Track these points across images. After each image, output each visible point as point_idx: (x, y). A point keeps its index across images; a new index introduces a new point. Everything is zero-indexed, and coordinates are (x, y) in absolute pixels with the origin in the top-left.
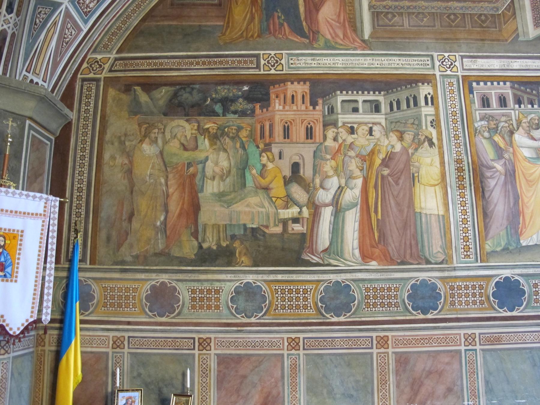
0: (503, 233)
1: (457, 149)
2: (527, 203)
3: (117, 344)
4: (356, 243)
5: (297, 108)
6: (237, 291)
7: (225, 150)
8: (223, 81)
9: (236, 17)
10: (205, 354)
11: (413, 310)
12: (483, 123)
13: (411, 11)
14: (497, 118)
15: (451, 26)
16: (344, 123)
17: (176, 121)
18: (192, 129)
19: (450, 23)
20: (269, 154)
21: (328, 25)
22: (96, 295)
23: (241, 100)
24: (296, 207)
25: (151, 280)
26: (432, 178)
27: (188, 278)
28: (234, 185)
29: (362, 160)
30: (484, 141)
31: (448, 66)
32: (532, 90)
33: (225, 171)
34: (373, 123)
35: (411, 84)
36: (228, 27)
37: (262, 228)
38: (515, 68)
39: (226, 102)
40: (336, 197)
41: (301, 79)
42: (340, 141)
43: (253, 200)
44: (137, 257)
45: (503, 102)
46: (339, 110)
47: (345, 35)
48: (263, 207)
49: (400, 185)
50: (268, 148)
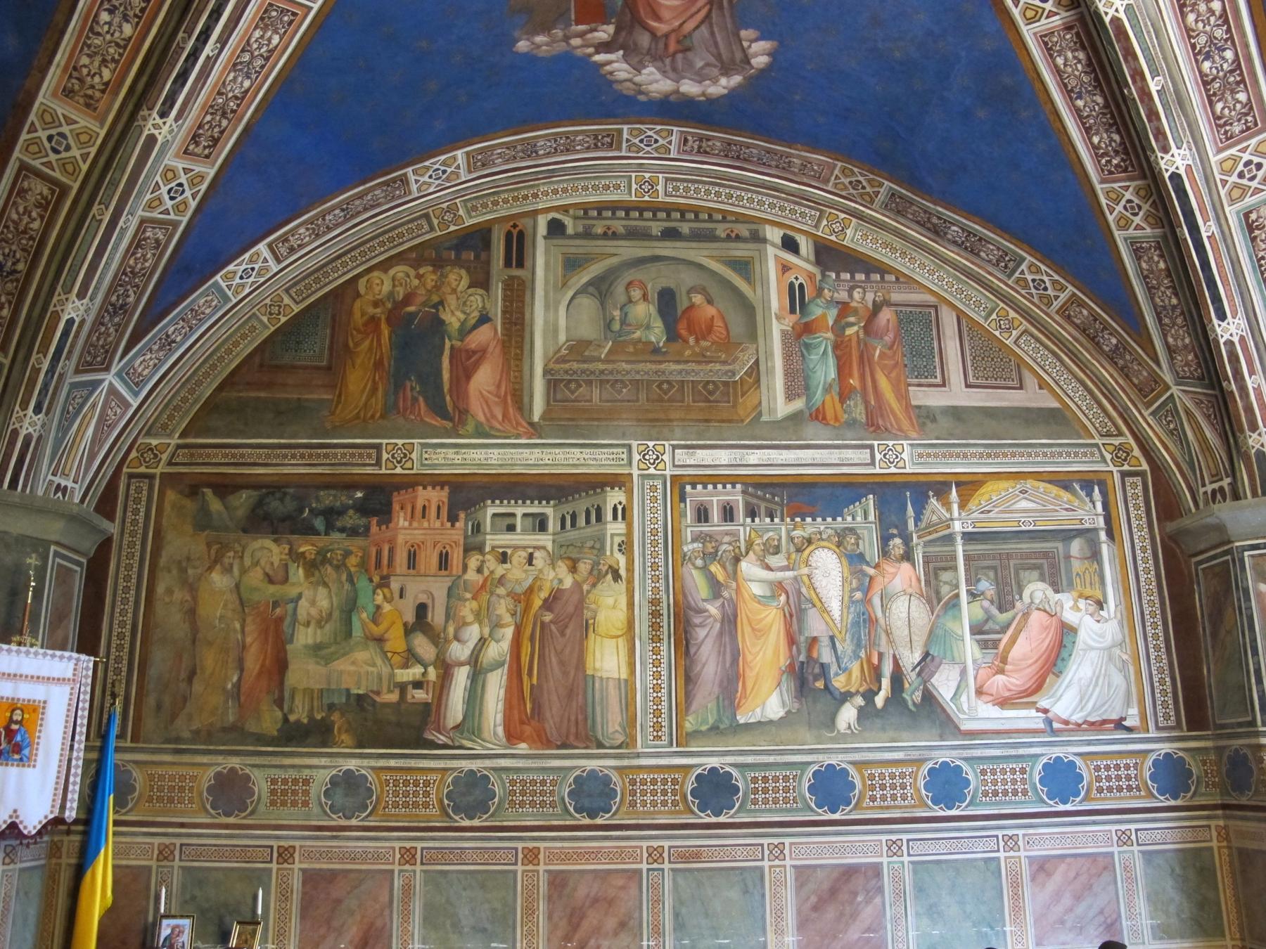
0: (712, 705)
3: (165, 854)
4: (500, 717)
6: (334, 782)
7: (325, 585)
10: (286, 869)
11: (576, 812)
12: (695, 545)
14: (718, 538)
16: (493, 548)
17: (260, 541)
18: (281, 553)
20: (386, 590)
22: (137, 786)
23: (351, 512)
25: (216, 764)
27: (266, 763)
28: (335, 634)
30: (694, 572)
31: (652, 461)
32: (774, 495)
34: (534, 548)
35: (594, 488)
36: (339, 402)
37: (371, 695)
38: (752, 462)
39: (331, 515)
40: (476, 652)
41: (437, 481)
42: (486, 572)
43: (361, 655)
44: (197, 732)
45: (728, 513)
46: (488, 529)
47: (505, 416)
48: (374, 665)
50: (384, 583)
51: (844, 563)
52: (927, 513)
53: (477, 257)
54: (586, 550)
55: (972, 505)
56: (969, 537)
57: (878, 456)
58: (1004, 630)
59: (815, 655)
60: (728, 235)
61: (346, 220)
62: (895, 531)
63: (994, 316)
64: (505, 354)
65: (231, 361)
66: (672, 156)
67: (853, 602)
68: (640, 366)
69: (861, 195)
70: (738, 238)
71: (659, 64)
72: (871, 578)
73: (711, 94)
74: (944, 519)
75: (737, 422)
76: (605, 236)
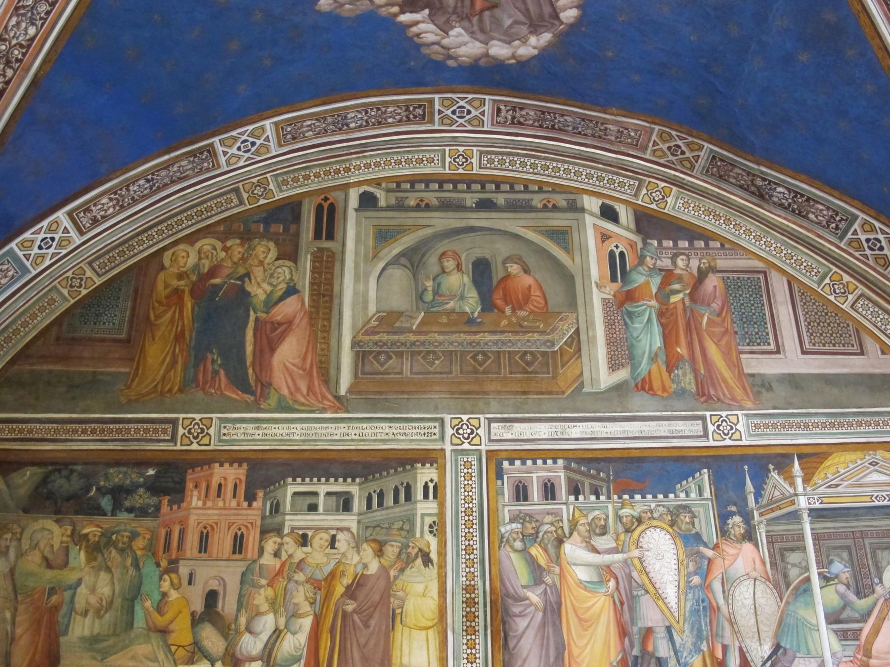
1: (468, 570)
2: (579, 655)
5: (224, 504)
7: (109, 570)
8: (118, 460)
9: (150, 360)
12: (514, 526)
13: (416, 349)
14: (538, 517)
15: (476, 372)
16: (293, 529)
17: (41, 521)
18: (63, 535)
19: (474, 367)
20: (173, 576)
21: (286, 372)
23: (141, 490)
24: (206, 661)
26: (423, 616)
28: (115, 624)
29: (315, 588)
30: (513, 556)
31: (466, 436)
33: (104, 603)
34: (338, 529)
35: (404, 466)
36: (136, 374)
39: (119, 493)
40: (269, 646)
41: (235, 458)
42: (284, 556)
45: (549, 491)
47: (310, 389)
49: (371, 628)
50: (172, 567)
51: (679, 544)
52: (768, 488)
53: (286, 230)
54: (394, 532)
55: (818, 479)
56: (817, 514)
57: (711, 428)
58: (865, 618)
59: (650, 648)
60: (545, 206)
61: (153, 193)
62: (734, 509)
63: (827, 280)
64: (312, 325)
65: (26, 334)
66: (485, 129)
67: (691, 588)
68: (454, 337)
69: (681, 162)
70: (555, 208)
71: (466, 23)
72: (710, 561)
73: (521, 56)
74: (788, 494)
75: (557, 393)
76: (418, 208)
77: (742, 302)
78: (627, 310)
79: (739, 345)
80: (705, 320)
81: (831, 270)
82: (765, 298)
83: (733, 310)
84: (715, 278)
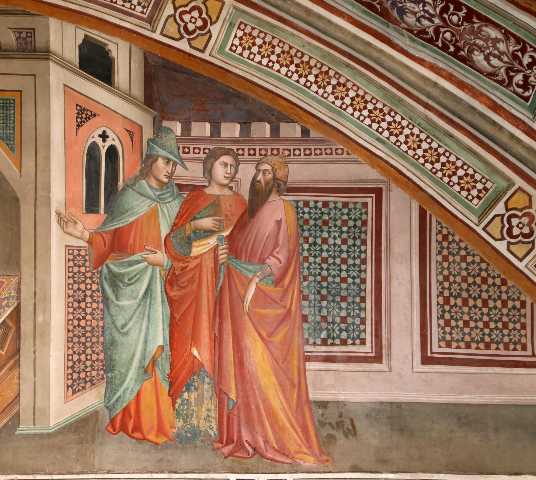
63: (500, 208)
77: (325, 254)
78: (110, 271)
79: (307, 342)
80: (252, 289)
81: (511, 184)
82: (369, 247)
83: (306, 273)
84: (281, 203)
